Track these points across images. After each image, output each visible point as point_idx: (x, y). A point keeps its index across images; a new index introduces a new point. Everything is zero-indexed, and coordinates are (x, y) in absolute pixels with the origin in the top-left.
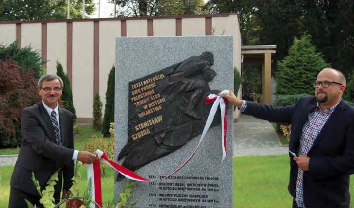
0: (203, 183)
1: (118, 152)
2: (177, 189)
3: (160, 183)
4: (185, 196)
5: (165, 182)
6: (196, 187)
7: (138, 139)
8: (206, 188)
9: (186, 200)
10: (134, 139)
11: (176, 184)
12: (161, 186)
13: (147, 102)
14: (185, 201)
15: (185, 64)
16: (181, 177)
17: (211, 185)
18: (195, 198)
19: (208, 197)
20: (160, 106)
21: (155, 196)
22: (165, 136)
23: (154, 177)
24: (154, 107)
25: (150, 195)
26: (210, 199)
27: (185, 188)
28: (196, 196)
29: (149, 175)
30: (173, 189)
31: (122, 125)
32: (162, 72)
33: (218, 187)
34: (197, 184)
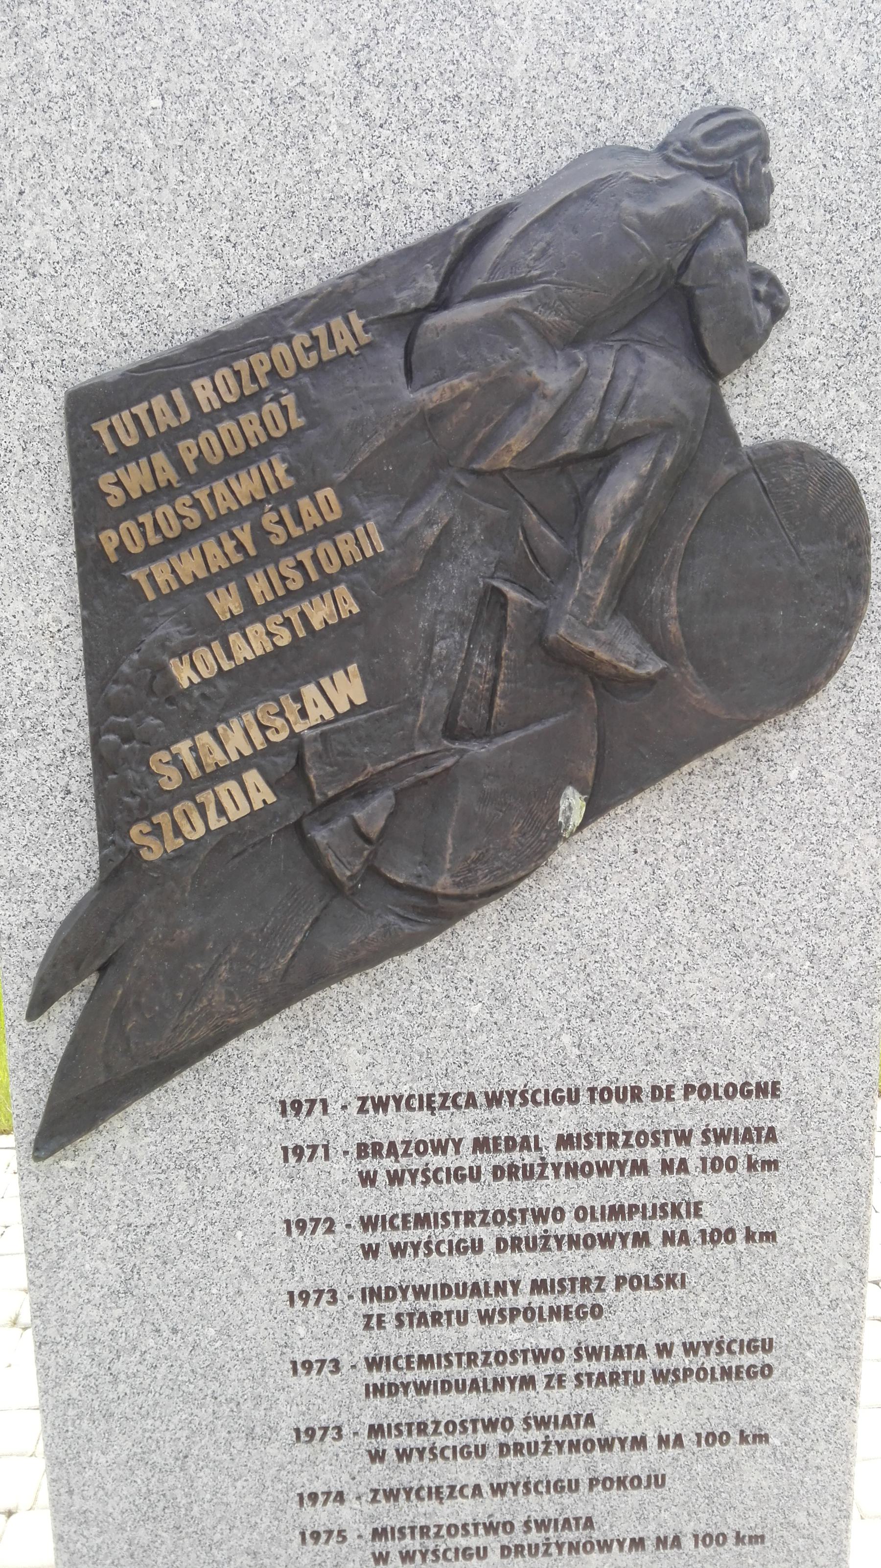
0: (672, 1124)
1: (28, 955)
2: (487, 1177)
4: (540, 1215)
5: (398, 1136)
6: (619, 1154)
7: (180, 855)
8: (694, 1153)
9: (553, 1243)
10: (153, 852)
11: (480, 1145)
12: (370, 1164)
13: (237, 558)
14: (546, 1248)
15: (543, 220)
16: (511, 1096)
17: (721, 1136)
18: (610, 1227)
19: (706, 1209)
20: (342, 590)
21: (330, 1231)
22: (392, 816)
23: (318, 1107)
24: (292, 597)
25: (289, 1232)
26: (715, 1224)
28: (616, 1212)
29: (277, 1095)
30: (457, 1175)
31: (46, 753)
32: (346, 294)
33: (774, 1146)
34: (628, 1134)
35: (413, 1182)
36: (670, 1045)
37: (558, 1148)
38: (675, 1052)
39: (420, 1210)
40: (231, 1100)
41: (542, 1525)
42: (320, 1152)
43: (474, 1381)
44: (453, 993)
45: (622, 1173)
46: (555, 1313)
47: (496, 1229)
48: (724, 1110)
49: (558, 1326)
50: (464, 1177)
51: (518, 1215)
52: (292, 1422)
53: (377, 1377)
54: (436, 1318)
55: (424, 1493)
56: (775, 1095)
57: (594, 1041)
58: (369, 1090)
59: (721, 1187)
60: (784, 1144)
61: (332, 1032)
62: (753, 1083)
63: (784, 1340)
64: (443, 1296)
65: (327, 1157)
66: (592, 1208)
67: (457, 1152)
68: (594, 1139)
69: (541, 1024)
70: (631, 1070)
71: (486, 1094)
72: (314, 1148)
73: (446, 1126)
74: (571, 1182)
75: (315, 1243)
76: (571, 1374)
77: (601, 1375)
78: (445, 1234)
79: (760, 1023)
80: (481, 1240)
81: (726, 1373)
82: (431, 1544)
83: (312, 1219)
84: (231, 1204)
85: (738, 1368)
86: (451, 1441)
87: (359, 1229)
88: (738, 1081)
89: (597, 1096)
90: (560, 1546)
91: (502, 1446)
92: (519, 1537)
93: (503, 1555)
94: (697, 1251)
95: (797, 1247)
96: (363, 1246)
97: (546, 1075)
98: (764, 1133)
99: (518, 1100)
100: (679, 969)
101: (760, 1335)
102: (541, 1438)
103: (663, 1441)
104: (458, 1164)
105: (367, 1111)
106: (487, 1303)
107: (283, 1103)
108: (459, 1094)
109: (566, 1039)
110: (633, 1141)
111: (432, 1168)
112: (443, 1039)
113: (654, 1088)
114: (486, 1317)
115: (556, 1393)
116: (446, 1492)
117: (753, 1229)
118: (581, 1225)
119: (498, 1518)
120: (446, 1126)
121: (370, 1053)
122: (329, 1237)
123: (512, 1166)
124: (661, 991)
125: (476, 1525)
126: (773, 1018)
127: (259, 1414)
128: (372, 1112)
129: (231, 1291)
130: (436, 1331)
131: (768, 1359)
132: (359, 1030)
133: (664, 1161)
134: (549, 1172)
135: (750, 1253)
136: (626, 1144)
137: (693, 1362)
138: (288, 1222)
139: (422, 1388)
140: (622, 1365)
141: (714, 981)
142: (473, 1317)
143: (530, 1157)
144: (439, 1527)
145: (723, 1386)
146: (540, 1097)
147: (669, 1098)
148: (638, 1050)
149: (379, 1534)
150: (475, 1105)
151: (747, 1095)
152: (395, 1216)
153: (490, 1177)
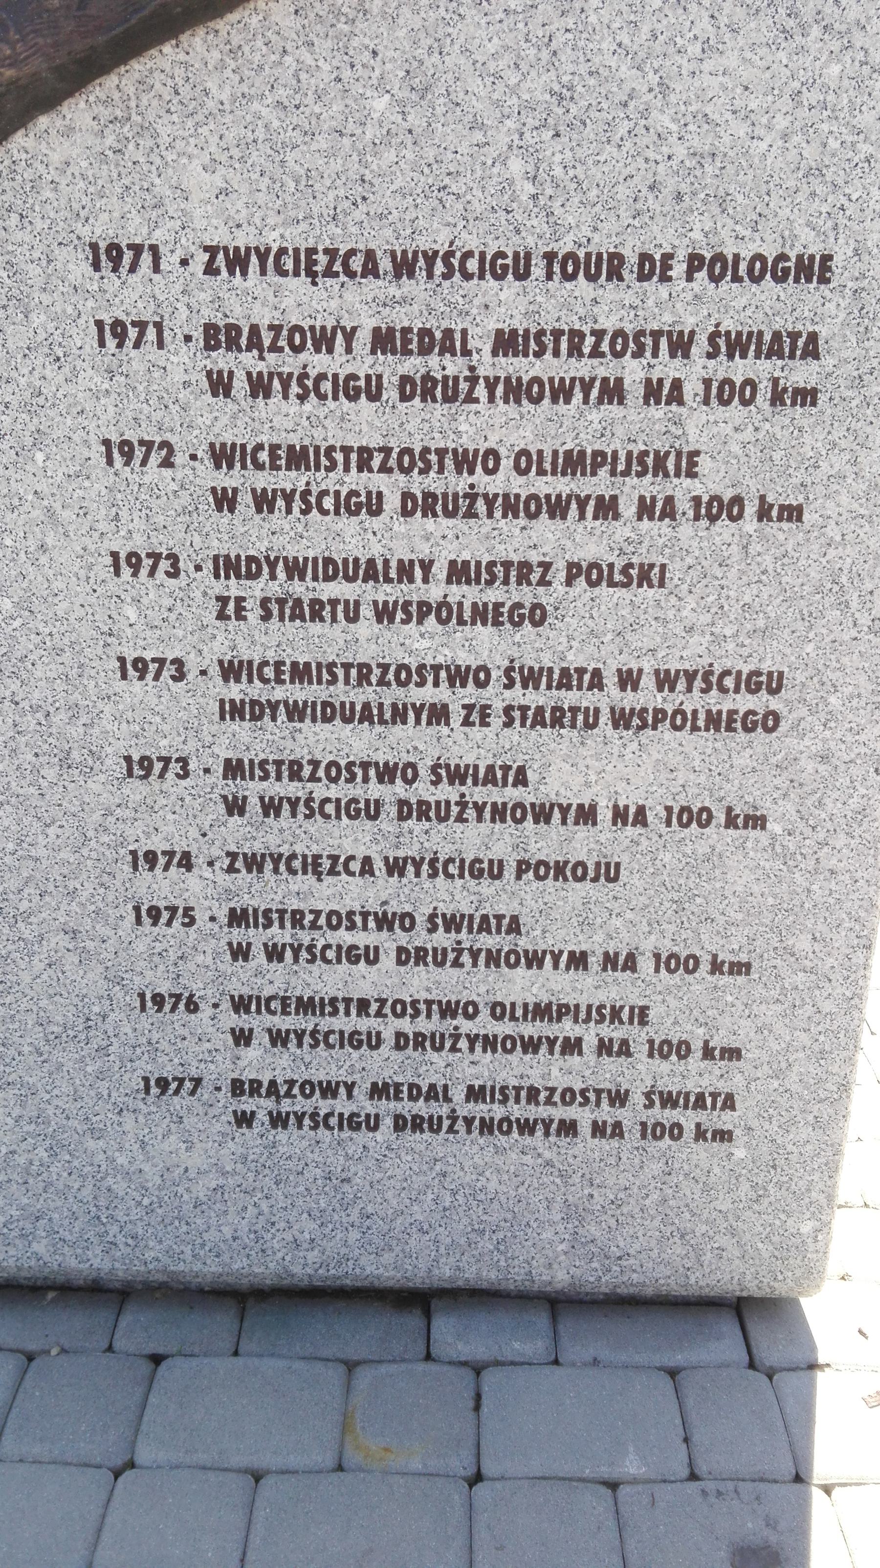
0: (665, 320)
2: (391, 394)
3: (211, 330)
5: (264, 318)
6: (582, 368)
9: (481, 506)
12: (222, 360)
14: (471, 514)
16: (430, 259)
18: (562, 485)
19: (704, 464)
21: (167, 463)
23: (146, 258)
25: (110, 462)
26: (716, 488)
27: (473, 380)
29: (85, 232)
33: (814, 365)
34: (599, 334)
35: (286, 397)
36: (670, 185)
37: (495, 353)
38: (679, 197)
39: (294, 440)
40: (19, 236)
41: (452, 923)
42: (151, 334)
43: (366, 706)
44: (346, 74)
45: (586, 401)
46: (480, 614)
47: (402, 478)
48: (744, 301)
49: (484, 633)
50: (358, 390)
51: (433, 458)
52: (121, 748)
53: (235, 691)
54: (317, 610)
55: (297, 864)
56: (824, 280)
57: (558, 171)
58: (219, 236)
59: (729, 429)
60: (828, 361)
61: (165, 131)
62: (793, 255)
63: (800, 677)
64: (327, 579)
65: (161, 345)
66: (540, 453)
67: (349, 350)
68: (548, 340)
69: (478, 136)
70: (610, 226)
71: (393, 254)
72: (141, 326)
73: (334, 304)
74: (511, 409)
75: (147, 479)
76: (498, 705)
77: (540, 710)
78: (329, 481)
79: (811, 152)
80: (380, 495)
81: (714, 721)
82: (305, 937)
83: (142, 443)
84: (26, 407)
85: (732, 713)
86: (333, 792)
87: (209, 463)
88: (770, 253)
89: (557, 268)
90: (475, 955)
91: (402, 803)
92: (420, 938)
93: (400, 962)
94: (686, 530)
95: (833, 532)
96: (214, 490)
97: (484, 226)
98: (801, 343)
99: (439, 268)
100: (695, 49)
101: (765, 667)
102: (454, 798)
103: (620, 815)
104: (349, 369)
105: (217, 272)
106: (387, 593)
107: (94, 247)
108: (352, 252)
109: (516, 166)
110: (605, 347)
111: (313, 373)
112: (330, 154)
113: (645, 257)
114: (384, 613)
115: (476, 732)
116: (326, 864)
117: (770, 499)
118: (522, 480)
119: (394, 907)
120: (334, 304)
121: (221, 171)
122: (167, 473)
123: (427, 378)
124: (664, 88)
125: (365, 915)
126: (833, 144)
127: (76, 731)
128: (224, 273)
129: (32, 544)
130: (316, 628)
131: (775, 704)
132: (204, 130)
133: (648, 381)
134: (481, 391)
135: (763, 538)
136: (596, 353)
137: (668, 701)
138: (107, 443)
139: (296, 712)
140: (569, 698)
141: (747, 74)
142: (366, 611)
143: (454, 366)
144: (317, 913)
145: (706, 740)
146: (472, 265)
147: (665, 278)
148: (623, 192)
149: (237, 918)
150: (377, 276)
151: (780, 278)
152: (259, 447)
153: (395, 395)
